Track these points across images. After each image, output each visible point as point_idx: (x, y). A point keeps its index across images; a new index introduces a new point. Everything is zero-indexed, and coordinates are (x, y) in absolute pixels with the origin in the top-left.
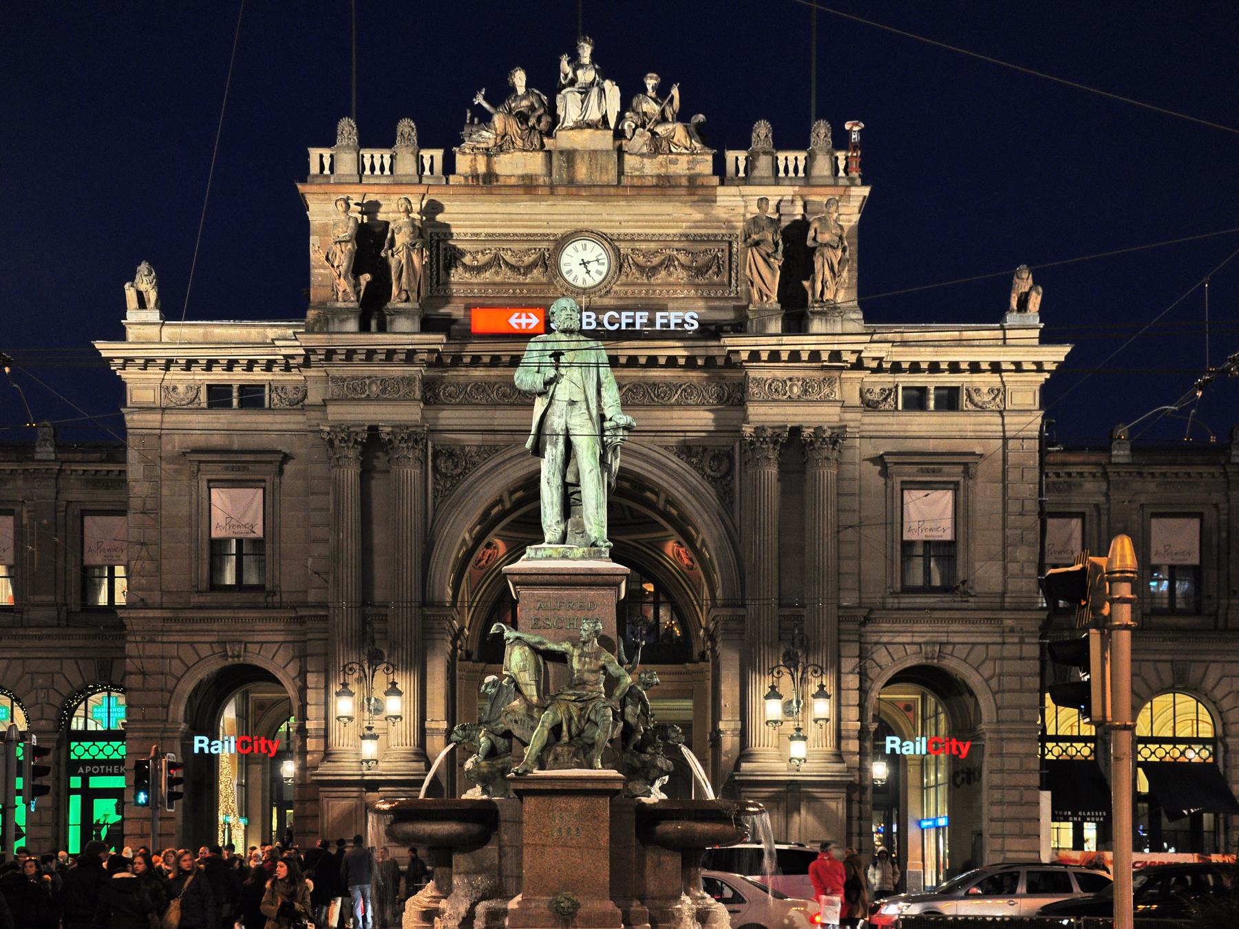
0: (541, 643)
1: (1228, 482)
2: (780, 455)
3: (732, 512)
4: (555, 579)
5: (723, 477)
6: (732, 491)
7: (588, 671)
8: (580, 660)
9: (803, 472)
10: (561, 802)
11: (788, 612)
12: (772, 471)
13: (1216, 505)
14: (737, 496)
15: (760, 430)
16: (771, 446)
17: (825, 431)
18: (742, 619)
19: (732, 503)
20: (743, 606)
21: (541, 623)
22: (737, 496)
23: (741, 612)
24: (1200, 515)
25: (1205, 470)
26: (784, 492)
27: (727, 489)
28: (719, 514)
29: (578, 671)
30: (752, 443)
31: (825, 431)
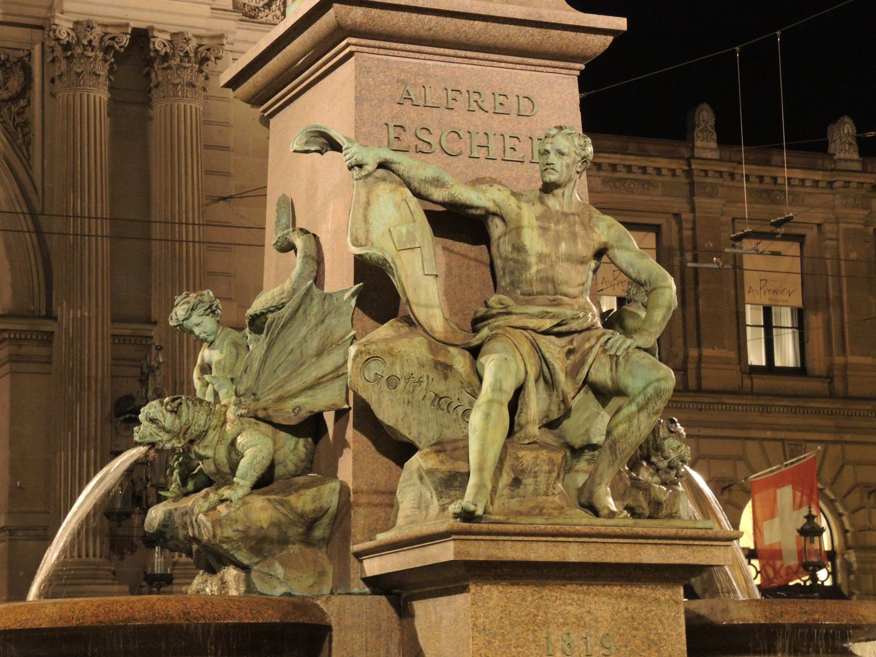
0: (437, 182)
1: (692, 184)
2: (111, 71)
3: (29, 158)
4: (449, 26)
5: (14, 99)
6: (26, 124)
7: (569, 258)
8: (544, 230)
9: (147, 103)
10: (564, 601)
11: (126, 329)
12: (101, 95)
13: (677, 216)
14: (38, 133)
15: (82, 26)
16: (100, 55)
17: (188, 41)
18: (48, 338)
19: (28, 144)
20: (50, 315)
21: (408, 139)
22: (38, 133)
23: (48, 326)
24: (656, 229)
25: (663, 163)
26: (116, 135)
27: (19, 120)
28: (6, 159)
29: (541, 257)
30: (67, 47)
31: (188, 41)
